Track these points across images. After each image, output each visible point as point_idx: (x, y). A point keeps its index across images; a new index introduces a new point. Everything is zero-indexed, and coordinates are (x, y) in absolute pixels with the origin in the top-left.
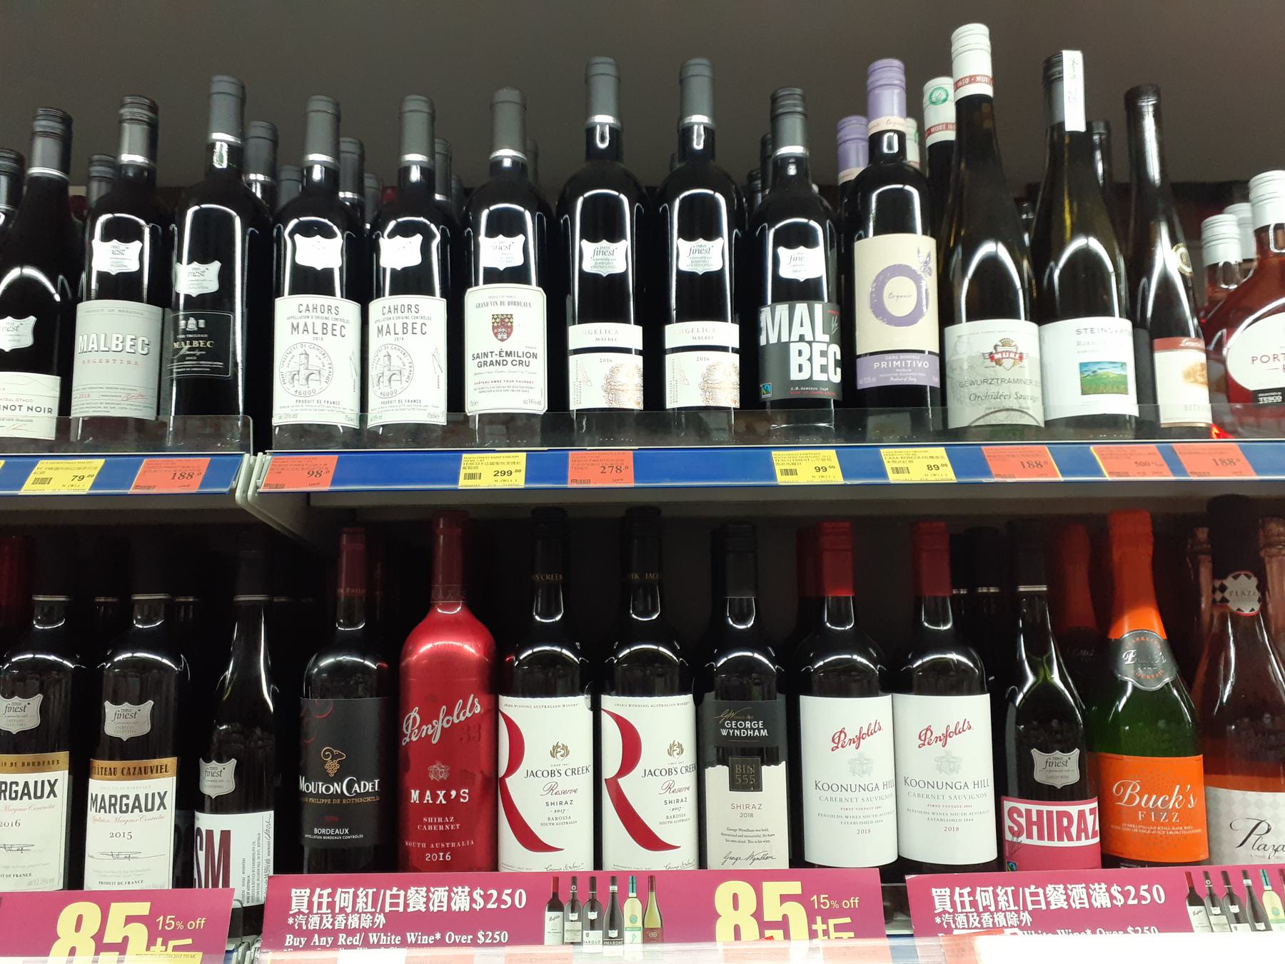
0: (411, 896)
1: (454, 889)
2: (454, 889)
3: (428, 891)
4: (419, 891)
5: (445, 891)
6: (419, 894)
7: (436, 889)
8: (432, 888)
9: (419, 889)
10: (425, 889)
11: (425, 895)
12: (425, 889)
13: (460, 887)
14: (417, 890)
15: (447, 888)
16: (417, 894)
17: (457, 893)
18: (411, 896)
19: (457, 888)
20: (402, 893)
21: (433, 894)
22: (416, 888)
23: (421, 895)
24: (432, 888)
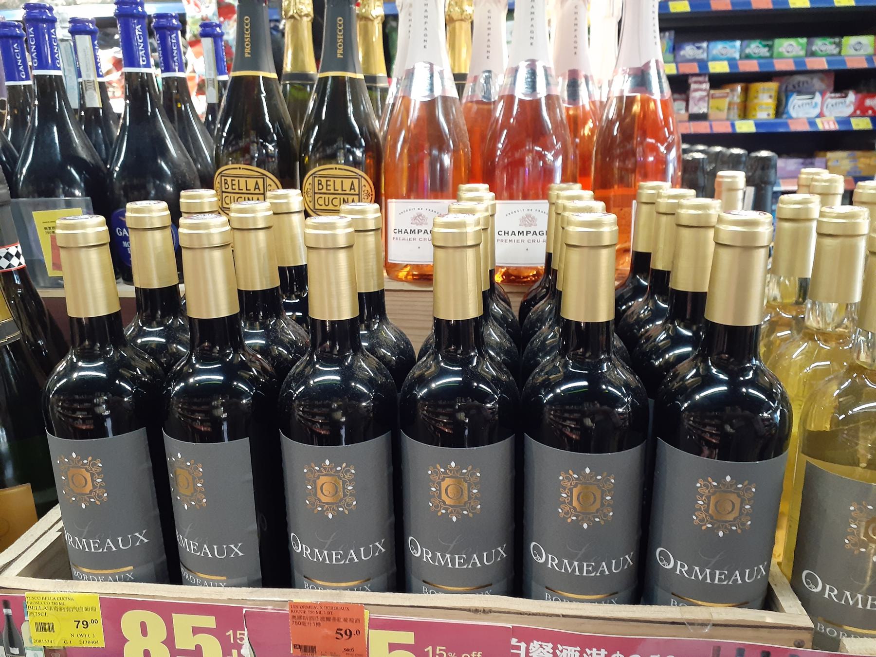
0: (534, 649)
1: (587, 650)
2: (587, 650)
3: (555, 648)
4: (543, 646)
5: (575, 651)
6: (544, 649)
7: (564, 647)
8: (559, 646)
9: (543, 644)
10: (550, 645)
11: (551, 651)
12: (550, 645)
13: (594, 650)
14: (541, 646)
15: (578, 649)
16: (541, 649)
17: (591, 654)
18: (534, 649)
19: (591, 649)
20: (523, 645)
21: (561, 651)
22: (540, 643)
23: (546, 650)
24: (559, 646)
